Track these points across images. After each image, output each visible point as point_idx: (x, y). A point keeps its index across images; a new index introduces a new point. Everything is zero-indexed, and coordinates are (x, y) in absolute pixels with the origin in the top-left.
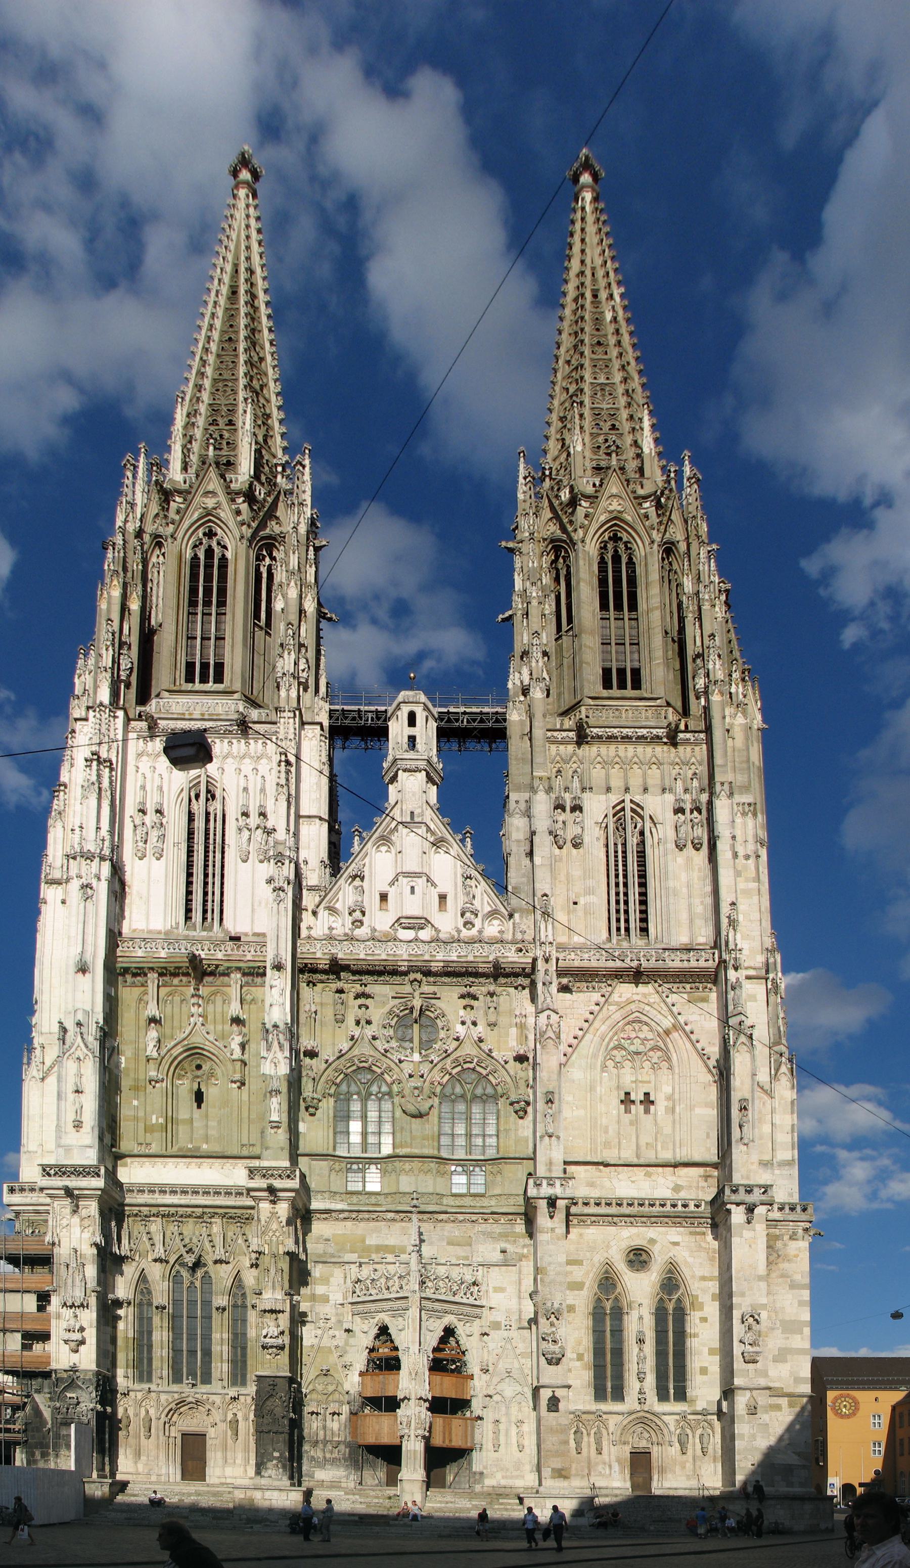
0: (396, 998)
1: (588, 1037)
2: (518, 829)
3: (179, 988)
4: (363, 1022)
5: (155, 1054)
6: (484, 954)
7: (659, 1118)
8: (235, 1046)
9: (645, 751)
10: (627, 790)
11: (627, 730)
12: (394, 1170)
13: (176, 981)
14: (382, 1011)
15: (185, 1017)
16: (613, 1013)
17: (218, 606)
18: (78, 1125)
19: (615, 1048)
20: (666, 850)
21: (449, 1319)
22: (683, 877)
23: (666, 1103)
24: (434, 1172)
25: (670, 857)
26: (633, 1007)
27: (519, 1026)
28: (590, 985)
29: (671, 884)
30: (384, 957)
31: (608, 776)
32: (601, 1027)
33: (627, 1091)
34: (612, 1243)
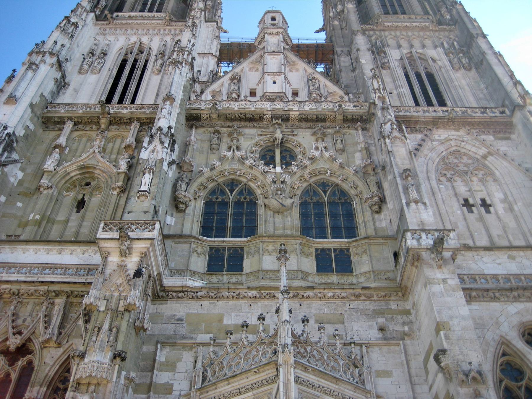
0: (261, 135)
2: (344, 62)
3: (88, 132)
4: (234, 147)
10: (412, 46)
13: (87, 129)
22: (463, 82)
23: (502, 205)
24: (299, 251)
25: (451, 73)
33: (466, 197)
34: (502, 319)
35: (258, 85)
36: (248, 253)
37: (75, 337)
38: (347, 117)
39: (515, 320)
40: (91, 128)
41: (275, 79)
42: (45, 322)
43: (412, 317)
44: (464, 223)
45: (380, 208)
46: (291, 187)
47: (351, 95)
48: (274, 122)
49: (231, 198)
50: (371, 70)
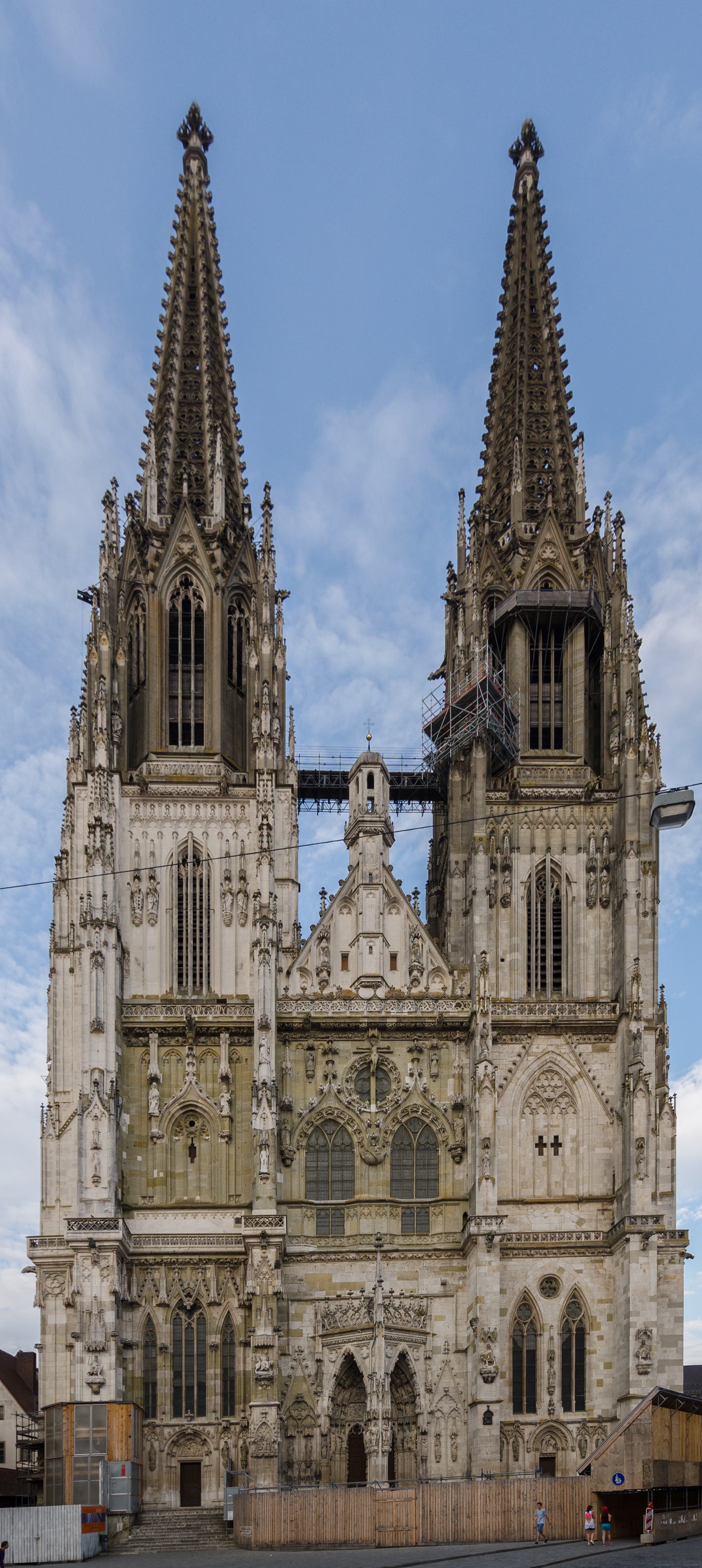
1: (512, 1085)
5: (156, 1112)
7: (566, 1159)
8: (224, 1103)
9: (565, 812)
10: (548, 849)
11: (552, 790)
12: (356, 1215)
15: (181, 1076)
16: (531, 1063)
17: (196, 663)
18: (97, 1180)
19: (532, 1096)
20: (579, 908)
21: (402, 1346)
25: (582, 914)
26: (547, 1057)
27: (457, 1076)
28: (513, 1037)
29: (582, 940)
31: (533, 836)
32: (522, 1077)
36: (349, 1216)
37: (229, 1297)
39: (539, 1274)
40: (178, 1041)
42: (205, 1286)
43: (467, 1273)
44: (531, 1167)
45: (461, 1158)
47: (456, 973)
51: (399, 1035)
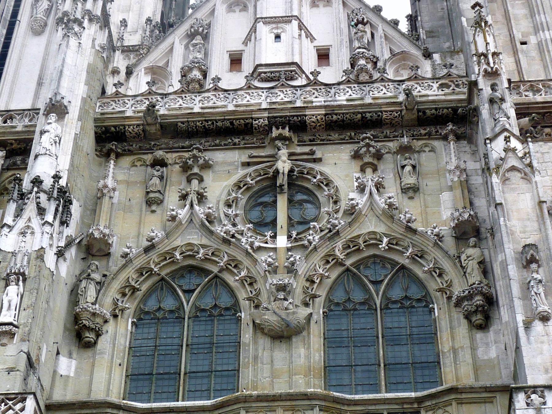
0: (248, 164)
6: (389, 94)
14: (226, 183)
30: (231, 108)
35: (245, 43)
38: (424, 113)
41: (279, 31)
46: (307, 280)
47: (436, 56)
48: (275, 133)
49: (187, 308)
50: (473, 7)
51: (335, 136)
